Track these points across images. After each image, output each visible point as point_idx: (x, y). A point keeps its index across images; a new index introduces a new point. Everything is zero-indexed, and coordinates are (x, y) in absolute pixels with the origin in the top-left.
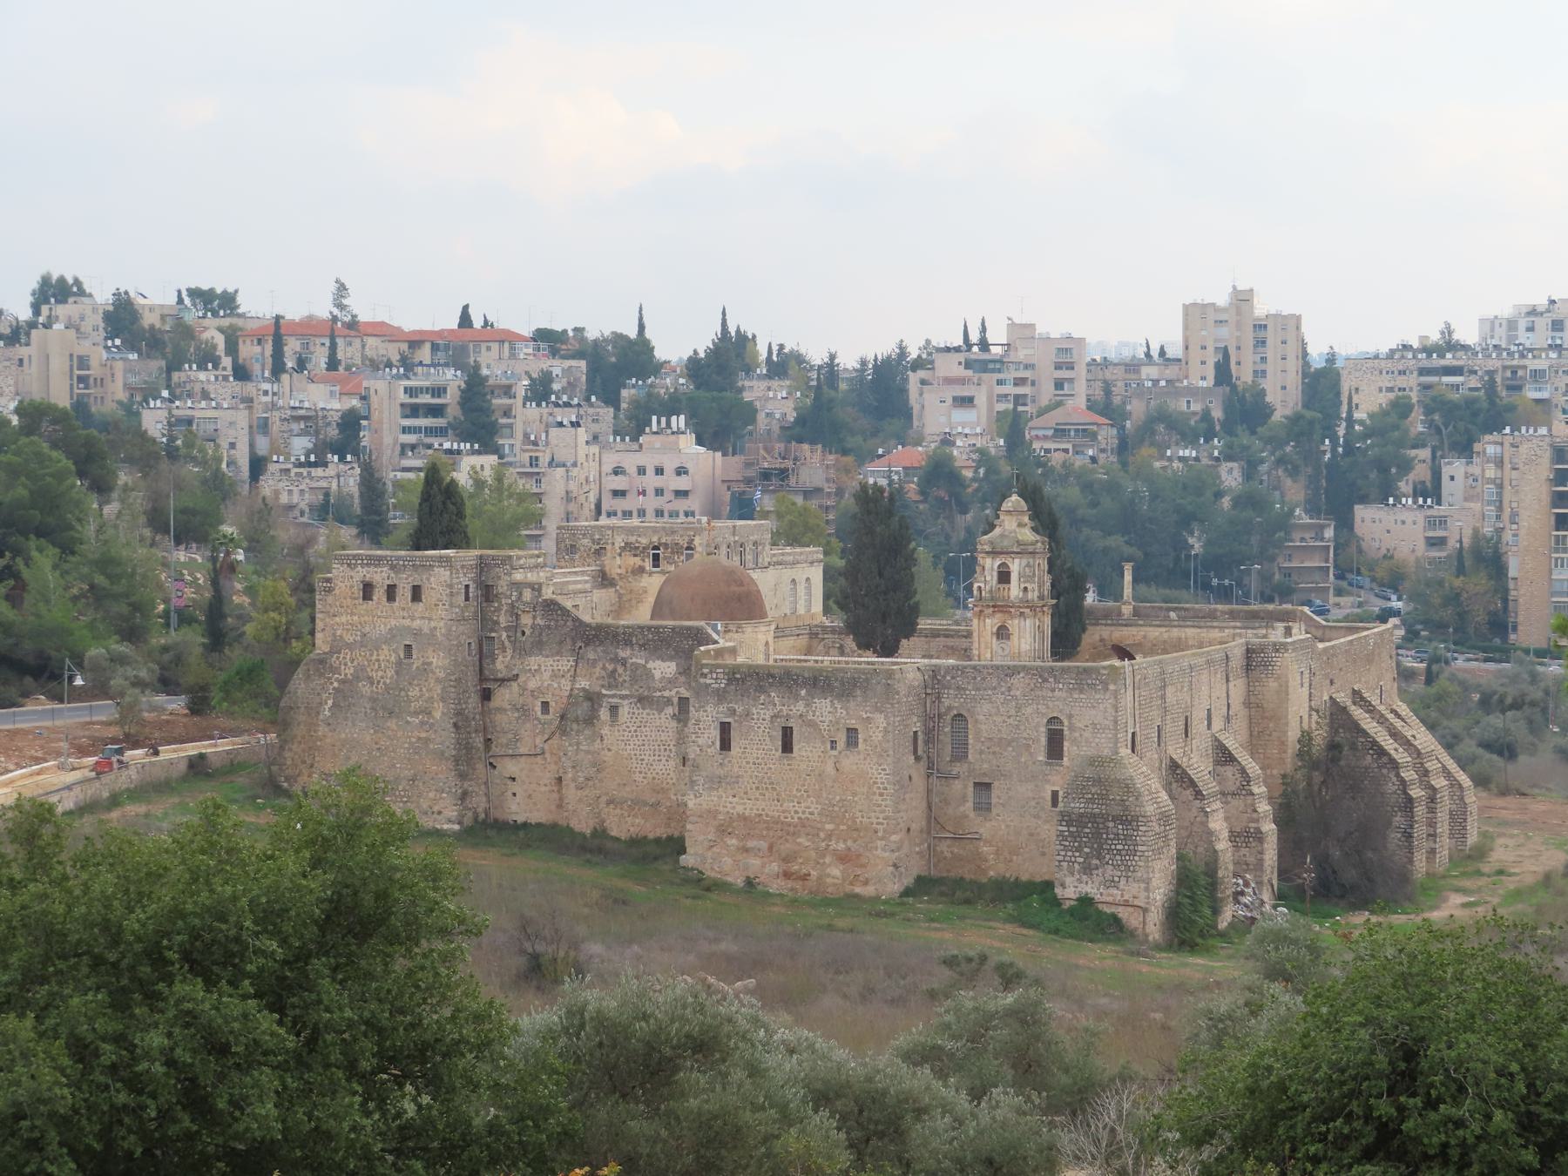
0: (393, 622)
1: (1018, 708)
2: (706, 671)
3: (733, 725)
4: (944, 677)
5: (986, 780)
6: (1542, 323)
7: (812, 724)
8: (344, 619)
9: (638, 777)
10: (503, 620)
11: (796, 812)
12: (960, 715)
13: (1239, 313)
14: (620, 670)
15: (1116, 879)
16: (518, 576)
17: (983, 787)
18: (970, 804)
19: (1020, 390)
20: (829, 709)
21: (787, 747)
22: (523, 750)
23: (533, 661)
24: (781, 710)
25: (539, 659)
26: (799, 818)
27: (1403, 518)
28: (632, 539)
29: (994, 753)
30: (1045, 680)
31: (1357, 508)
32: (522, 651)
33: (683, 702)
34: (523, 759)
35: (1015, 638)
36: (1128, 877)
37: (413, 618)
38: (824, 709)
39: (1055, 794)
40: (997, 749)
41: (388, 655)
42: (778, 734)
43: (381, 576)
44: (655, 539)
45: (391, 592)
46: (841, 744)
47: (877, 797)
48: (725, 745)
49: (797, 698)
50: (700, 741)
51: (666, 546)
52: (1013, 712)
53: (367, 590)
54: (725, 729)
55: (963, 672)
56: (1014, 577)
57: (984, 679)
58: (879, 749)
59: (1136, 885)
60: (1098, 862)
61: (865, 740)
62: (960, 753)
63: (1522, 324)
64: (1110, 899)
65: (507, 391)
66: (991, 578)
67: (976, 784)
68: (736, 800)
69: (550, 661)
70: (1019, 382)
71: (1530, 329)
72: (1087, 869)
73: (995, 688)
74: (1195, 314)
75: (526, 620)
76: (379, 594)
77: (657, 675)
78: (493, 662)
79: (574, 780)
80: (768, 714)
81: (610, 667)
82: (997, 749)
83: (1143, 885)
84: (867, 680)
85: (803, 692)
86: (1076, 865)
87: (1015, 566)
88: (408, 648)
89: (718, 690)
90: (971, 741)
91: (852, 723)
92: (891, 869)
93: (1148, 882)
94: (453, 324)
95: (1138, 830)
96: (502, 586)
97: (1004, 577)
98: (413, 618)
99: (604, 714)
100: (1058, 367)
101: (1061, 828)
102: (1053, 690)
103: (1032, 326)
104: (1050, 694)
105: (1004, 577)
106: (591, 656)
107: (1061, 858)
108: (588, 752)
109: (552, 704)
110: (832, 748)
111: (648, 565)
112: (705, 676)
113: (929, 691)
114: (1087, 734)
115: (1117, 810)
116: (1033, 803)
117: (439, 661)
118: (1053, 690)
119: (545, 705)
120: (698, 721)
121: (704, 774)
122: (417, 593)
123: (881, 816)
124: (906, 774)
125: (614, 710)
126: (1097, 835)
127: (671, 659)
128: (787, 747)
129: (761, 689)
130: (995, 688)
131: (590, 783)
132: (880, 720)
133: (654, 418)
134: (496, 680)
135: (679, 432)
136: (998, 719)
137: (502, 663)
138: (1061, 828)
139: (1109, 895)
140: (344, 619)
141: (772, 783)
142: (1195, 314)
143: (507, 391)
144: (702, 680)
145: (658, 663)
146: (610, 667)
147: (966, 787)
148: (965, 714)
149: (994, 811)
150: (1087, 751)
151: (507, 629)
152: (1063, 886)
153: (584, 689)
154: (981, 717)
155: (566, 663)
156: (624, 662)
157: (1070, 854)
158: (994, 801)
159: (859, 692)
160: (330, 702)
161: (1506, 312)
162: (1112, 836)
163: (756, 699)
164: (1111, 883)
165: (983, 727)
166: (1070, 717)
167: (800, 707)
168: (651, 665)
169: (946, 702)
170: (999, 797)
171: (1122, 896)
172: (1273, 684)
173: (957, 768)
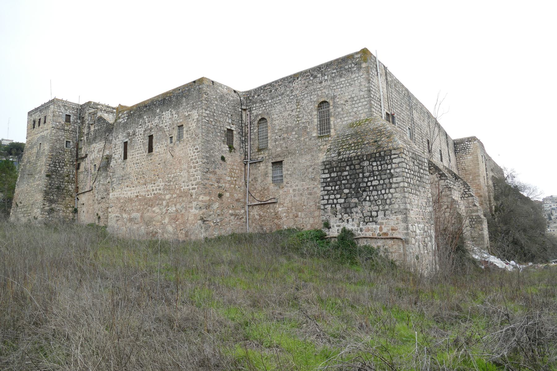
1: (298, 103)
3: (129, 142)
4: (253, 97)
5: (279, 159)
11: (153, 190)
12: (263, 119)
15: (374, 214)
17: (278, 164)
18: (270, 179)
20: (170, 116)
21: (150, 150)
22: (86, 190)
26: (154, 194)
29: (284, 139)
30: (315, 77)
32: (90, 143)
34: (87, 194)
36: (385, 211)
40: (285, 135)
42: (147, 141)
49: (155, 115)
52: (295, 106)
55: (264, 90)
59: (393, 217)
60: (356, 200)
61: (187, 131)
64: (369, 234)
72: (347, 209)
73: (283, 94)
82: (285, 135)
83: (400, 217)
84: (189, 90)
86: (338, 207)
88: (41, 144)
90: (269, 135)
92: (200, 222)
93: (405, 212)
95: (391, 163)
101: (324, 176)
107: (326, 202)
108: (103, 185)
109: (97, 165)
110: (171, 142)
113: (244, 107)
114: (347, 107)
115: (372, 149)
116: (310, 170)
118: (321, 83)
121: (116, 176)
123: (194, 183)
124: (218, 155)
126: (354, 176)
128: (150, 150)
129: (140, 116)
130: (283, 94)
131: (104, 200)
132: (195, 114)
136: (286, 114)
138: (324, 176)
139: (368, 230)
148: (266, 117)
149: (285, 180)
150: (348, 120)
157: (332, 197)
158: (284, 173)
160: (20, 175)
162: (367, 174)
164: (371, 219)
166: (334, 97)
169: (254, 112)
170: (288, 170)
171: (381, 229)
172: (470, 158)
173: (264, 155)
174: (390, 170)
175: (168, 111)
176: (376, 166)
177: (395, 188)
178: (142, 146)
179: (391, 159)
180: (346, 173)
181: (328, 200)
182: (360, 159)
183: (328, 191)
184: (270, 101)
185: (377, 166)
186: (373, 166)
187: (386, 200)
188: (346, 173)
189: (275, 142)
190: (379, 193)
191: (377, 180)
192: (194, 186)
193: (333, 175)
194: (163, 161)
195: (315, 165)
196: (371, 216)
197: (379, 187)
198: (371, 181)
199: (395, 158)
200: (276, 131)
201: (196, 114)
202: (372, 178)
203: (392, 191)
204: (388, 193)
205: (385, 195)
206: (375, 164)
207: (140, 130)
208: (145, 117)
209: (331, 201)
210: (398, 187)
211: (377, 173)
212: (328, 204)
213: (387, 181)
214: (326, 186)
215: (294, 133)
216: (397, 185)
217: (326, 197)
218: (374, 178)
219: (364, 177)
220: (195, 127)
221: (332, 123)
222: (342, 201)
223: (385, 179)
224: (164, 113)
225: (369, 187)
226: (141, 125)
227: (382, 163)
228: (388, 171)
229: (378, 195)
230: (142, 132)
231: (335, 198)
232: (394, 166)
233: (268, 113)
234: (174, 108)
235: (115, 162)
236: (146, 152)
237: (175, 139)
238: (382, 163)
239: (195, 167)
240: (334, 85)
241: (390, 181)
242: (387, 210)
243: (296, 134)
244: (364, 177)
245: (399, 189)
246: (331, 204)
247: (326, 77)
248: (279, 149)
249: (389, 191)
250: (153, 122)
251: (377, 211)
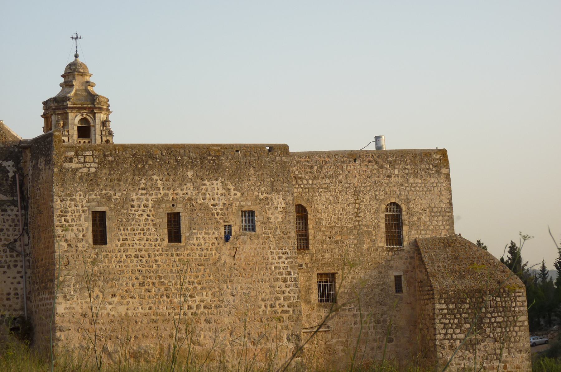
1: (357, 195)
2: (71, 154)
7: (204, 208)
11: (190, 307)
15: (498, 351)
20: (221, 191)
24: (166, 195)
29: (336, 242)
30: (382, 167)
31: (117, 140)
39: (398, 279)
47: (280, 283)
49: (184, 180)
50: (70, 235)
52: (352, 200)
57: (321, 168)
58: (278, 232)
60: (479, 337)
68: (115, 299)
72: (469, 345)
73: (332, 177)
80: (151, 200)
82: (338, 238)
85: (190, 174)
86: (458, 342)
89: (88, 175)
91: (249, 205)
102: (389, 176)
104: (386, 180)
112: (70, 160)
116: (377, 290)
118: (389, 176)
121: (74, 272)
123: (286, 303)
130: (332, 177)
132: (278, 200)
136: (338, 207)
141: (160, 277)
144: (67, 165)
147: (309, 279)
148: (304, 204)
154: (321, 207)
157: (450, 331)
159: (252, 171)
163: (134, 183)
165: (324, 216)
167: (188, 190)
174: (514, 307)
175: (217, 180)
176: (500, 302)
177: (519, 327)
178: (151, 227)
179: (516, 297)
180: (467, 306)
181: (446, 334)
182: (481, 292)
183: (445, 324)
184: (310, 182)
185: (501, 302)
186: (497, 302)
187: (510, 338)
188: (467, 306)
189: (322, 243)
190: (504, 330)
191: (501, 316)
192: (286, 308)
193: (451, 306)
194: (211, 261)
195: (383, 284)
196: (495, 354)
197: (504, 324)
198: (495, 318)
199: (519, 296)
200: (323, 229)
201: (281, 200)
202: (496, 315)
203: (516, 329)
204: (513, 331)
205: (509, 333)
206: (498, 299)
207: (144, 197)
208: (155, 177)
209: (449, 336)
210: (522, 326)
211: (501, 309)
212: (444, 339)
213: (511, 319)
214: (442, 318)
215: (352, 237)
216: (521, 324)
217: (443, 331)
218: (498, 314)
219: (487, 312)
220: (280, 219)
221: (405, 233)
222: (463, 336)
223: (510, 316)
224: (206, 182)
225: (493, 323)
226: (143, 189)
227: (506, 299)
228: (513, 309)
229: (501, 332)
230: (150, 203)
231: (454, 333)
232: (518, 304)
233: (308, 200)
234: (231, 177)
235: (65, 245)
236: (162, 240)
237: (235, 230)
238: (506, 299)
239: (285, 280)
240: (407, 185)
241: (514, 319)
242: (512, 348)
243: (355, 239)
244: (487, 312)
245: (523, 328)
246: (449, 340)
247: (396, 172)
248: (328, 256)
249: (513, 329)
250: (179, 191)
251: (501, 349)
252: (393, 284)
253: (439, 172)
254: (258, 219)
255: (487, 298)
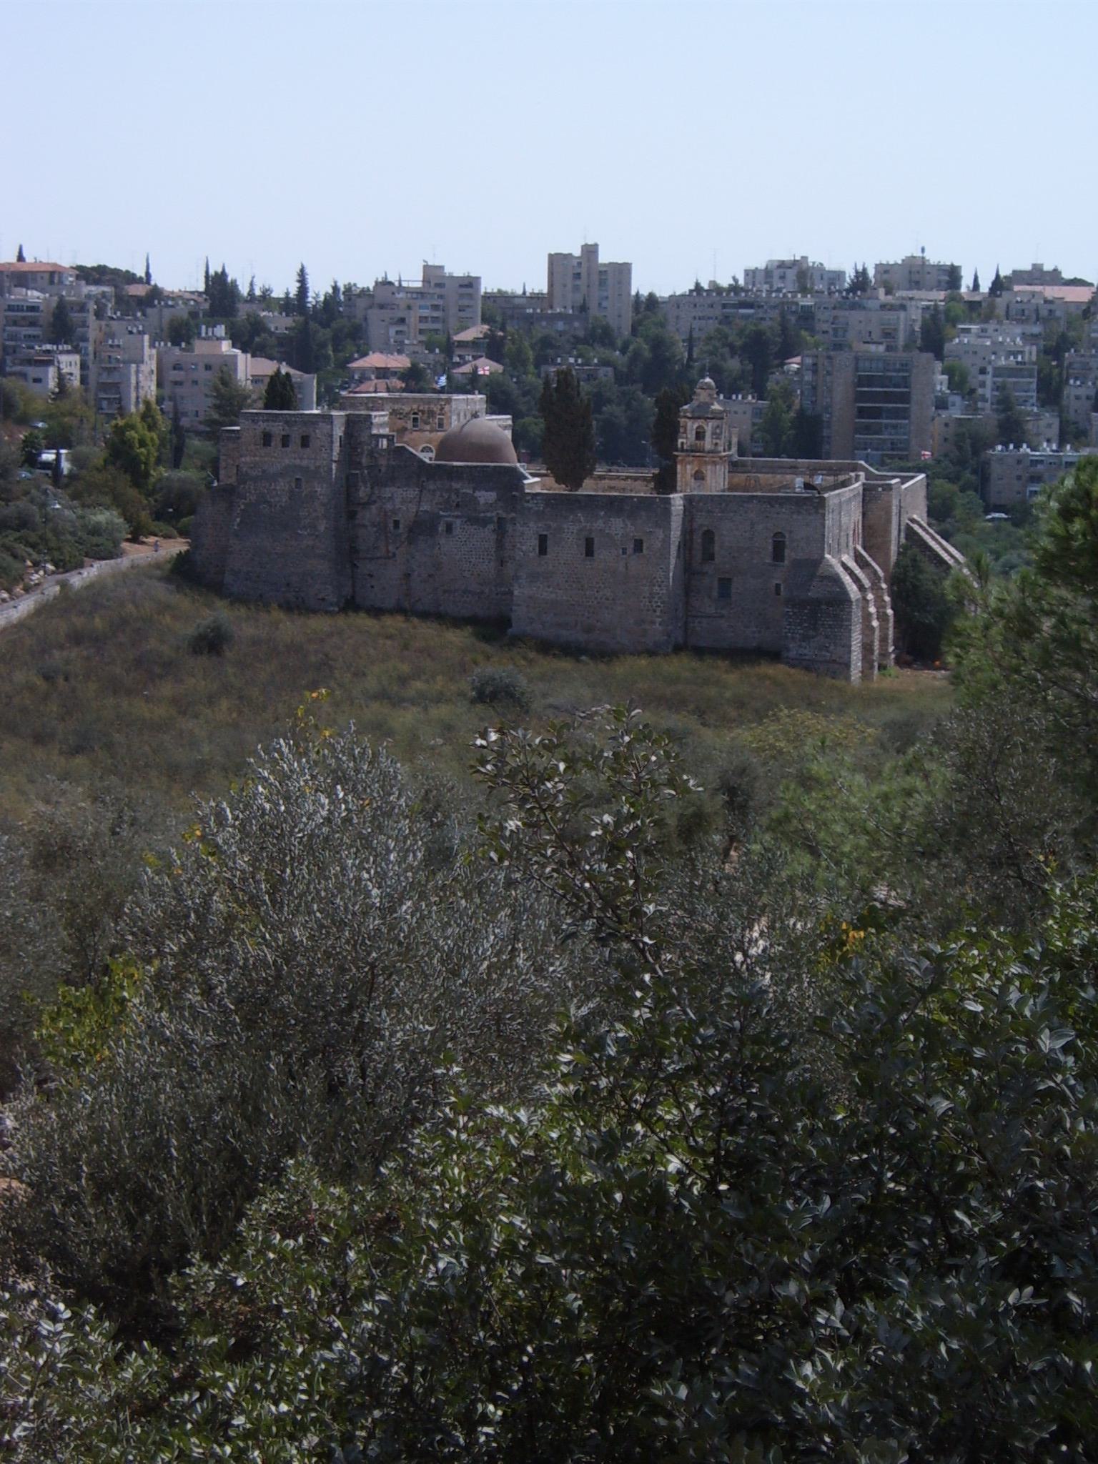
0: (287, 461)
5: (727, 576)
6: (791, 274)
8: (248, 459)
9: (466, 574)
10: (365, 461)
13: (589, 260)
14: (454, 497)
16: (375, 431)
19: (435, 314)
21: (589, 552)
23: (387, 492)
25: (393, 489)
27: (735, 409)
28: (396, 407)
33: (501, 521)
35: (708, 478)
37: (301, 459)
38: (618, 526)
39: (778, 586)
41: (282, 485)
42: (583, 542)
43: (277, 429)
44: (415, 406)
45: (285, 441)
46: (630, 551)
48: (543, 550)
51: (423, 412)
53: (267, 439)
54: (543, 540)
56: (708, 435)
62: (708, 556)
63: (777, 274)
65: (82, 308)
66: (691, 436)
67: (720, 579)
69: (400, 491)
70: (435, 307)
71: (783, 277)
72: (805, 638)
74: (556, 262)
75: (383, 462)
76: (276, 442)
77: (482, 501)
78: (357, 490)
79: (419, 575)
81: (446, 495)
87: (709, 427)
91: (638, 535)
94: (14, 259)
96: (364, 438)
97: (700, 435)
98: (301, 459)
99: (441, 528)
100: (462, 296)
103: (442, 268)
105: (700, 435)
106: (431, 486)
109: (402, 521)
110: (624, 553)
111: (410, 425)
117: (321, 489)
119: (396, 523)
120: (523, 534)
122: (305, 442)
125: (449, 528)
127: (491, 490)
128: (589, 552)
133: (204, 327)
134: (359, 504)
135: (219, 339)
137: (363, 492)
140: (248, 459)
142: (556, 262)
143: (82, 308)
145: (483, 493)
146: (446, 495)
151: (369, 467)
152: (788, 650)
153: (426, 511)
155: (412, 493)
156: (457, 492)
158: (733, 590)
161: (761, 265)
166: (791, 532)
167: (600, 524)
168: (477, 494)
252: (773, 589)
253: (817, 512)
254: (645, 546)
255: (824, 607)
